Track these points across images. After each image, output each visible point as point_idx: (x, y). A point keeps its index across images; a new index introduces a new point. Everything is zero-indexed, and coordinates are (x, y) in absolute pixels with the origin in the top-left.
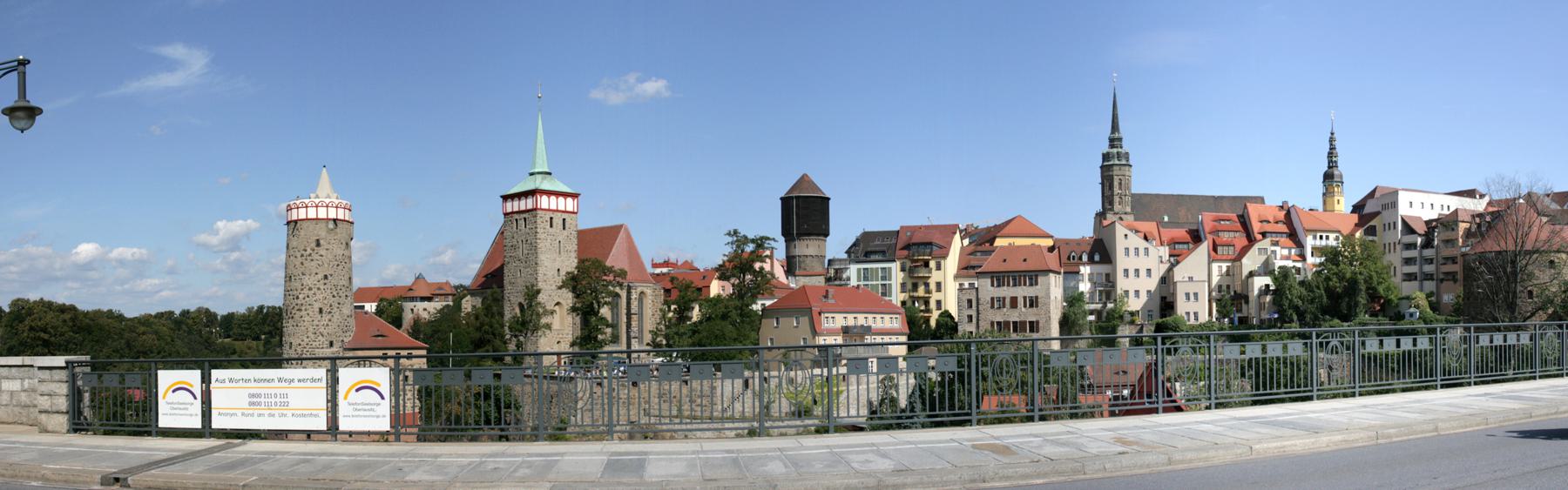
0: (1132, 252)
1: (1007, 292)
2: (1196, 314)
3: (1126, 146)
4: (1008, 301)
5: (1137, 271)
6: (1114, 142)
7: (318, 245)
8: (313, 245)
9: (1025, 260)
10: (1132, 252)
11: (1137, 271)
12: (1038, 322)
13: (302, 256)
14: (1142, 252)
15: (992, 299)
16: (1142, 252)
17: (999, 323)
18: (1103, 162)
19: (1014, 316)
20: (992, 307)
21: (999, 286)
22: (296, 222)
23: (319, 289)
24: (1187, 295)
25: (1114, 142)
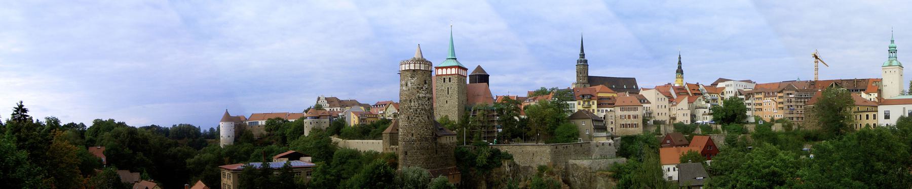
0: (660, 99)
1: (626, 113)
2: (687, 121)
3: (586, 58)
4: (627, 116)
5: (662, 106)
6: (583, 55)
7: (425, 83)
8: (424, 83)
9: (631, 102)
10: (660, 99)
11: (662, 106)
12: (638, 124)
13: (418, 88)
14: (663, 99)
15: (621, 116)
16: (663, 99)
17: (623, 124)
18: (578, 63)
19: (629, 122)
20: (621, 118)
21: (623, 111)
22: (414, 71)
23: (426, 105)
24: (684, 115)
25: (583, 55)
